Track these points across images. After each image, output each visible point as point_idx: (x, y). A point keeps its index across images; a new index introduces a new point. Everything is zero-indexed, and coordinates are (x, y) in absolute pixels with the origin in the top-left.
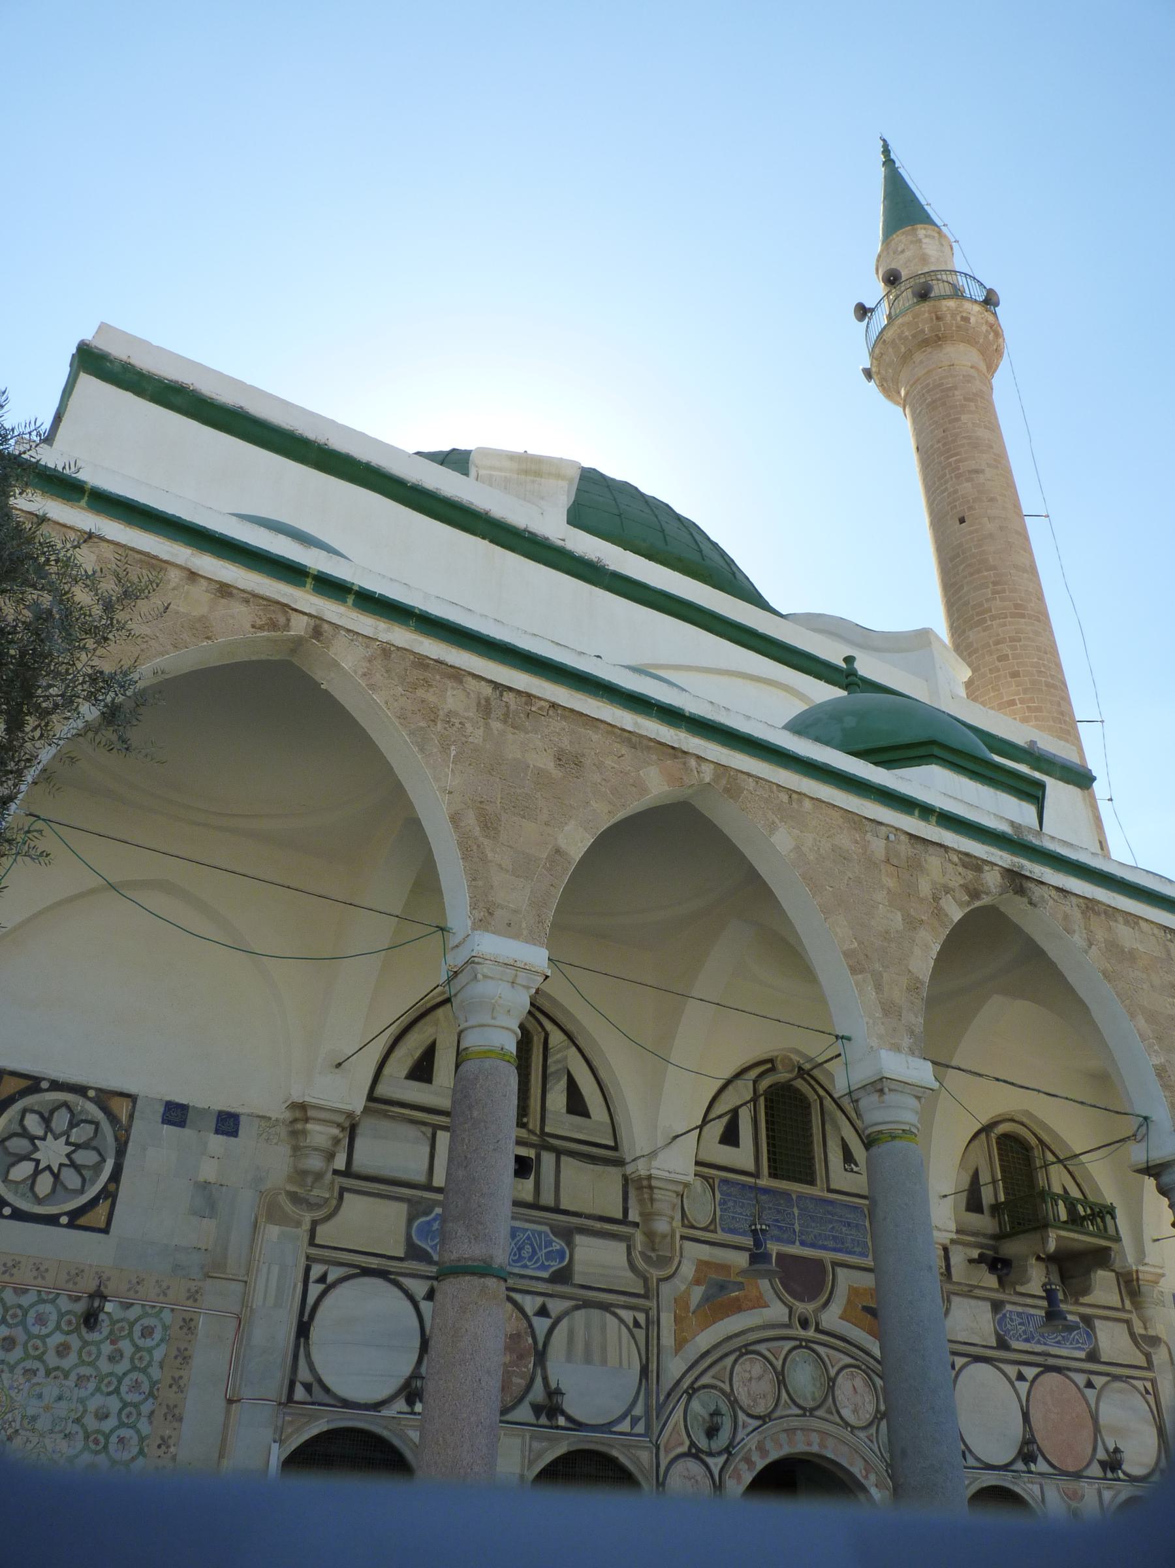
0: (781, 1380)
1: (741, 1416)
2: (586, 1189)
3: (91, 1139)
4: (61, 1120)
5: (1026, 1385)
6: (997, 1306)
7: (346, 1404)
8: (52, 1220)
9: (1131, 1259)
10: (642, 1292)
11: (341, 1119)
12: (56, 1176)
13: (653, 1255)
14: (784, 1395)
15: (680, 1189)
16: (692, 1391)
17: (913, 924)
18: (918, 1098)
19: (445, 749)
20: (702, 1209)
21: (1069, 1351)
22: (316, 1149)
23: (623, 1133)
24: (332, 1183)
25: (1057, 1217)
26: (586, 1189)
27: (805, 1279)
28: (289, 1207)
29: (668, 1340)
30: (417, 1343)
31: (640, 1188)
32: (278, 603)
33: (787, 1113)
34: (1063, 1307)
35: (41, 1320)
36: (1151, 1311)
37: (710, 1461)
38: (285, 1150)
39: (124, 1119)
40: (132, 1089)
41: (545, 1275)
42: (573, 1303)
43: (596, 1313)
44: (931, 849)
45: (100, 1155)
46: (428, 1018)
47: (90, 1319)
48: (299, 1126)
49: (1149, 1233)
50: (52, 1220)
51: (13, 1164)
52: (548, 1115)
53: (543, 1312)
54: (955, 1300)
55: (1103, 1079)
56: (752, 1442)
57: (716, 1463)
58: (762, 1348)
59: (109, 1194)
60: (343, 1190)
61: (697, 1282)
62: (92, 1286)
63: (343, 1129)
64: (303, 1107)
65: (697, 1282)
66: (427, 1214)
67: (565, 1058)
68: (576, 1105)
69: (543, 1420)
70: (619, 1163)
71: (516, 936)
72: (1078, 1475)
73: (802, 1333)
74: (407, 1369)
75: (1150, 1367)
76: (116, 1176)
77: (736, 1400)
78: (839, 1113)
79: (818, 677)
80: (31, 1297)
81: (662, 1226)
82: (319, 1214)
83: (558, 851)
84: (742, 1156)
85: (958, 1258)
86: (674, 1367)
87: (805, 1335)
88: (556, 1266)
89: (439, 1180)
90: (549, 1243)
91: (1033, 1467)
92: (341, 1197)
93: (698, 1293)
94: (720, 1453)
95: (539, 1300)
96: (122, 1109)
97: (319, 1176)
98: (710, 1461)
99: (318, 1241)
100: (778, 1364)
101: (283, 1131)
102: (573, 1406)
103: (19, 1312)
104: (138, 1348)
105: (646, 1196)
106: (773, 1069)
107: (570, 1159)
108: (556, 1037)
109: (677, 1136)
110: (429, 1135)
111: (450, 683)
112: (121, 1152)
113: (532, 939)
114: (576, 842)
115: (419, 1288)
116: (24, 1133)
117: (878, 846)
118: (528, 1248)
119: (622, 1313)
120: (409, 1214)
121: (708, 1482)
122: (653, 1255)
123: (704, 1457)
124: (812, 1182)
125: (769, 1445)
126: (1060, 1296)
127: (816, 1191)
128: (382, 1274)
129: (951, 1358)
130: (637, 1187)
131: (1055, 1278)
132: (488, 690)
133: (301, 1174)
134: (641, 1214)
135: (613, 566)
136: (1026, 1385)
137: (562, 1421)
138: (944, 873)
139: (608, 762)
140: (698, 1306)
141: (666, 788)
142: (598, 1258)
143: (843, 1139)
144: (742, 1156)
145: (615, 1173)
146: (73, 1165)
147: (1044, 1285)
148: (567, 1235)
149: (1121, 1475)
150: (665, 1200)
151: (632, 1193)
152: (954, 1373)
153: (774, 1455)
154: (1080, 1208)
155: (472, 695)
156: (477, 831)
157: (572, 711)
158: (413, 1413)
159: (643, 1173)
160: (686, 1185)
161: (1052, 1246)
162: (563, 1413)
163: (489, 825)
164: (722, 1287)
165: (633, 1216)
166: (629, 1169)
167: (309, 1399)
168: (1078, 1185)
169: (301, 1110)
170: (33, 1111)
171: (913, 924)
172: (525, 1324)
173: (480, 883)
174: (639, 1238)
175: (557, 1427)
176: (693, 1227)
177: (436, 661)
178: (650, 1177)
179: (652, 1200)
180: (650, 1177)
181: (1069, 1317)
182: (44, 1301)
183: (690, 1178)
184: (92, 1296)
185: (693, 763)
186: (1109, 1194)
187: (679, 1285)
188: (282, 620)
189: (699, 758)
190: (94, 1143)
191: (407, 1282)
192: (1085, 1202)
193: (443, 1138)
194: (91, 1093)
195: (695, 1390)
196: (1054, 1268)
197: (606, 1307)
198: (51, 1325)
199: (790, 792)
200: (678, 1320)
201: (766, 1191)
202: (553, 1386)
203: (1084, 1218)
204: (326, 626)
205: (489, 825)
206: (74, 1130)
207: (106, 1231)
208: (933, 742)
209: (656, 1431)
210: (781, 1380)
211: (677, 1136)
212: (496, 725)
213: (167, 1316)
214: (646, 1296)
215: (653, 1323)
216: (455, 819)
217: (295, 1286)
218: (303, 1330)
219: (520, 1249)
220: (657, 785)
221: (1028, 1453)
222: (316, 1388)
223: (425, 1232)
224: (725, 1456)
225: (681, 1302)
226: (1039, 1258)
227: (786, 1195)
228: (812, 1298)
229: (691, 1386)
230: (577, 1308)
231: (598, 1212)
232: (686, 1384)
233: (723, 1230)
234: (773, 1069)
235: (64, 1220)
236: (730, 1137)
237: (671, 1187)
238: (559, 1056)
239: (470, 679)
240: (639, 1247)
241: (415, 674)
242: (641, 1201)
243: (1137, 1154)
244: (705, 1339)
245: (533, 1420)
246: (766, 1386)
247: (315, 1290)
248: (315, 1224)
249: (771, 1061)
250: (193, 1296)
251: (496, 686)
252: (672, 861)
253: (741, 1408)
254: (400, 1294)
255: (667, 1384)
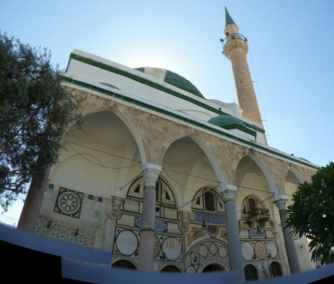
0: (209, 250)
1: (201, 257)
2: (170, 214)
3: (76, 201)
4: (71, 197)
5: (254, 245)
6: (249, 231)
7: (123, 255)
8: (69, 215)
9: (272, 219)
10: (181, 234)
11: (122, 200)
12: (70, 207)
13: (183, 226)
14: (209, 252)
15: (188, 213)
16: (191, 253)
17: (233, 160)
18: (234, 193)
19: (140, 127)
20: (193, 217)
21: (262, 237)
22: (117, 205)
23: (177, 203)
24: (120, 212)
25: (259, 213)
26: (170, 214)
27: (213, 230)
28: (112, 216)
29: (186, 243)
30: (137, 244)
31: (181, 213)
32: (108, 99)
33: (209, 197)
34: (260, 229)
35: (68, 233)
36: (275, 228)
37: (195, 266)
38: (111, 205)
39: (82, 198)
40: (83, 192)
41: (162, 231)
42: (168, 236)
43: (172, 238)
44: (236, 145)
45: (77, 204)
46: (138, 180)
47: (76, 234)
48: (114, 201)
49: (275, 214)
50: (69, 215)
51: (63, 204)
52: (162, 199)
53: (162, 238)
54: (241, 231)
55: (267, 187)
56: (203, 262)
57: (196, 267)
58: (205, 244)
59: (79, 211)
60: (122, 213)
61: (192, 231)
62: (76, 228)
63: (122, 201)
64: (114, 197)
65: (192, 231)
66: (138, 219)
67: (165, 188)
68: (168, 197)
69: (162, 259)
70: (176, 208)
71: (155, 164)
72: (263, 260)
73: (212, 240)
74: (135, 249)
75: (275, 238)
76: (80, 208)
77: (200, 254)
78: (219, 197)
79: (214, 112)
80: (66, 229)
81: (185, 221)
82: (117, 218)
83: (163, 147)
84: (201, 206)
85: (242, 223)
86: (188, 248)
87: (213, 240)
88: (164, 229)
89: (141, 212)
90: (163, 225)
91: (256, 260)
92: (122, 215)
93: (192, 234)
94: (197, 265)
95: (161, 236)
96: (81, 196)
97: (117, 210)
98: (195, 266)
99: (117, 223)
100: (208, 247)
101: (110, 201)
102: (168, 257)
103: (64, 231)
104: (85, 241)
105: (182, 215)
106: (206, 189)
107: (167, 208)
108: (163, 184)
109: (187, 203)
110: (139, 203)
111: (141, 114)
112: (81, 204)
113: (158, 165)
114: (167, 145)
115: (137, 233)
116: (64, 199)
117: (226, 145)
118: (158, 225)
119: (177, 238)
120: (135, 218)
121: (195, 271)
122: (183, 226)
123: (194, 266)
124: (214, 211)
125: (206, 263)
126: (260, 227)
127: (215, 212)
128: (130, 230)
129: (240, 242)
130: (180, 213)
131: (259, 224)
132: (149, 115)
133: (114, 210)
134: (181, 219)
135: (173, 90)
136: (254, 245)
137: (166, 260)
138: (238, 150)
139: (173, 129)
140: (192, 236)
141: (185, 134)
142: (173, 228)
143: (220, 202)
144: (201, 206)
145: (175, 211)
146: (73, 205)
147: (257, 226)
148: (166, 223)
149: (271, 258)
150: (185, 216)
151: (179, 215)
152: (241, 245)
153: (207, 264)
154: (263, 211)
155: (146, 116)
156: (147, 143)
157: (166, 119)
158: (136, 257)
159: (181, 210)
160: (190, 212)
161: (258, 218)
162: (166, 258)
163: (149, 142)
164: (197, 232)
165: (179, 219)
166: (178, 210)
167: (116, 254)
168: (263, 206)
169: (114, 198)
170: (66, 195)
171: (233, 160)
172: (158, 241)
173: (148, 153)
174: (180, 223)
175: (165, 261)
176: (191, 221)
177: (139, 110)
178: (182, 211)
179: (183, 216)
180: (182, 211)
181: (262, 231)
182: (68, 230)
183: (190, 211)
184: (76, 230)
185: (190, 129)
186: (268, 208)
187: (189, 232)
188: (109, 103)
189: (191, 128)
190: (76, 202)
191: (135, 232)
192: (264, 209)
193: (141, 204)
194: (76, 192)
195: (192, 253)
196: (259, 222)
197: (174, 237)
198: (70, 234)
199: (209, 134)
200: (188, 239)
201: (205, 213)
202: (164, 253)
203: (264, 213)
204: (117, 103)
205: (149, 142)
206: (73, 199)
207: (79, 218)
208: (236, 125)
209: (184, 261)
210: (209, 250)
211: (187, 203)
212: (151, 122)
213: (90, 235)
214: (182, 235)
215: (183, 240)
216: (143, 141)
217: (113, 232)
218: (115, 240)
219: (157, 226)
220: (183, 134)
221: (255, 257)
222: (117, 251)
223: (138, 222)
224: (198, 265)
225: (189, 235)
226: (256, 221)
227: (209, 213)
228: (214, 234)
229: (191, 252)
230: (168, 237)
231: (172, 218)
232: (190, 252)
233: (197, 221)
234: (206, 189)
235: (71, 215)
236: (198, 203)
237: (187, 213)
238: (164, 188)
239: (145, 113)
240: (180, 225)
241: (134, 112)
242: (181, 216)
243: (273, 200)
244: (194, 243)
245: (160, 259)
246: (206, 251)
247: (117, 233)
248: (117, 220)
249: (206, 187)
250: (95, 232)
251: (150, 114)
252: (186, 148)
253: (201, 256)
254: (134, 234)
255: (186, 251)
